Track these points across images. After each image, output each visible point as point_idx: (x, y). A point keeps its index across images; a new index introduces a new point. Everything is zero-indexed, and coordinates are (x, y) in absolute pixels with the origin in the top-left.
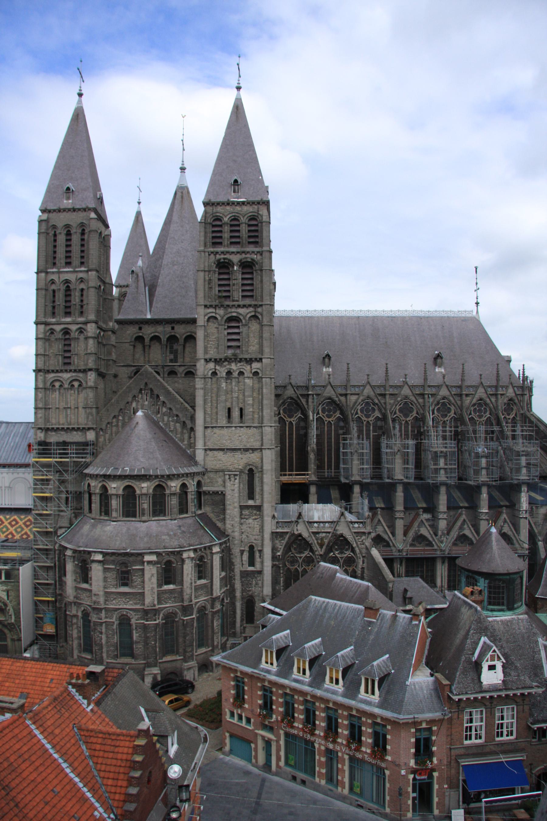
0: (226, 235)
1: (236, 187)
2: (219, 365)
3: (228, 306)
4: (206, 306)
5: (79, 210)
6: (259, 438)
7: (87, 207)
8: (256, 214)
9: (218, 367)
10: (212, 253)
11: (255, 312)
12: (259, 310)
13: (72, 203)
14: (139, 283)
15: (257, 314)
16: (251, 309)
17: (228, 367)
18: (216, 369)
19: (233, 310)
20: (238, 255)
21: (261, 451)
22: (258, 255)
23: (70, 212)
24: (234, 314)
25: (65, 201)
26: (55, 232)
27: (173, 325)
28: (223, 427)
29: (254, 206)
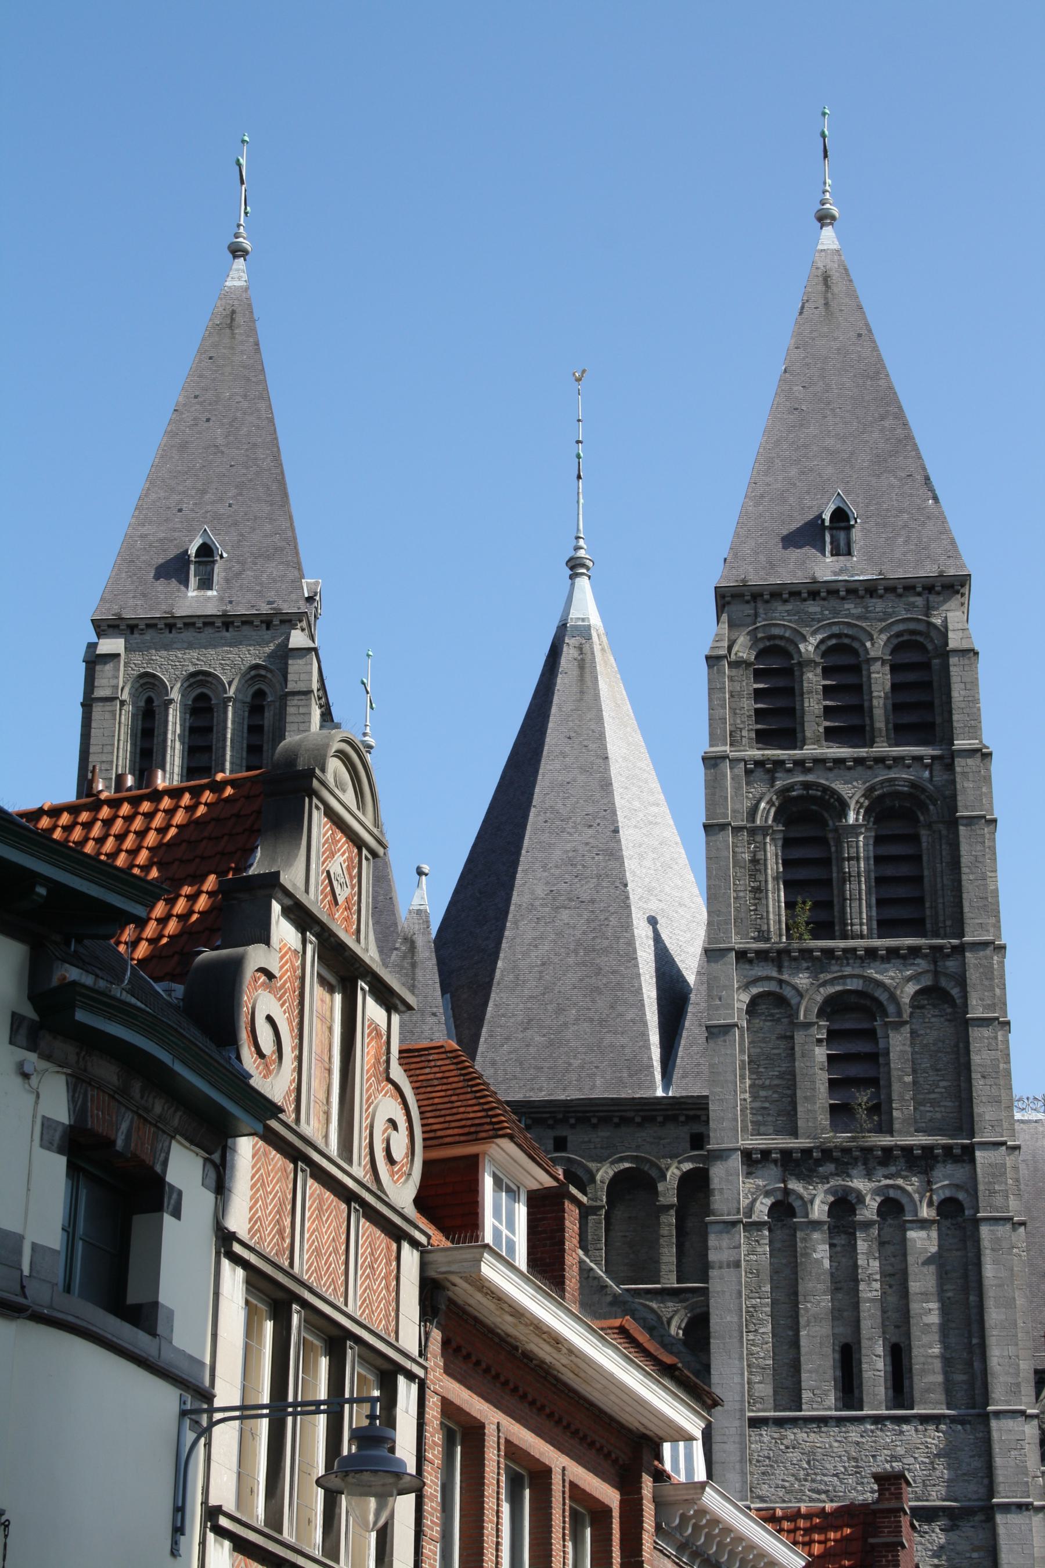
0: (813, 704)
1: (842, 535)
2: (799, 1177)
3: (829, 953)
4: (742, 956)
5: (247, 621)
6: (977, 1463)
7: (278, 613)
8: (921, 627)
9: (794, 1185)
10: (759, 763)
11: (936, 974)
12: (951, 965)
13: (221, 599)
14: (419, 973)
15: (944, 983)
16: (922, 964)
17: (836, 1182)
18: (787, 1192)
19: (848, 971)
20: (860, 769)
21: (990, 1520)
22: (937, 767)
23: (209, 630)
24: (852, 985)
25: (192, 593)
26: (149, 701)
27: (562, 1132)
28: (823, 1421)
29: (912, 599)
